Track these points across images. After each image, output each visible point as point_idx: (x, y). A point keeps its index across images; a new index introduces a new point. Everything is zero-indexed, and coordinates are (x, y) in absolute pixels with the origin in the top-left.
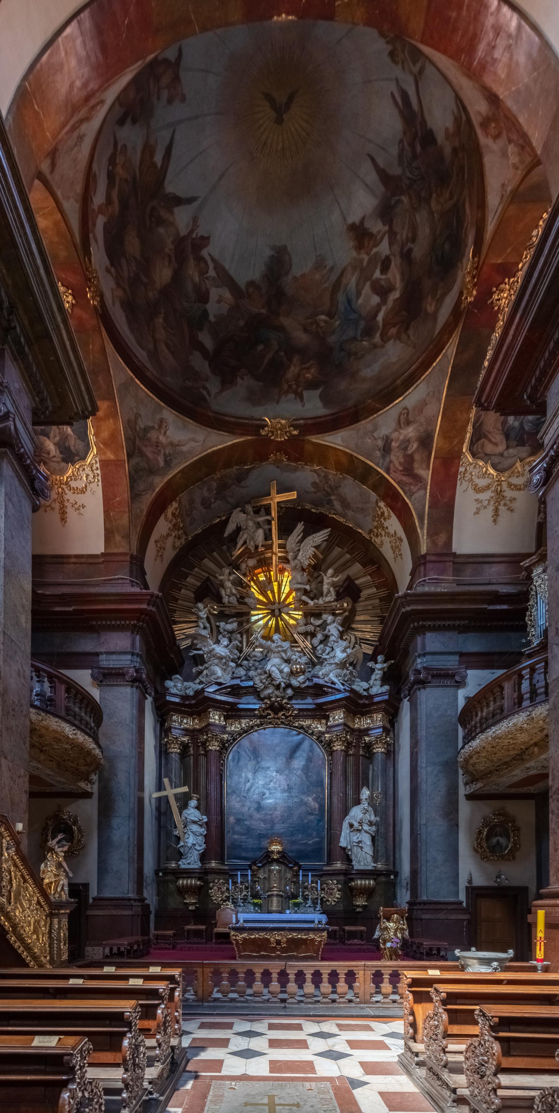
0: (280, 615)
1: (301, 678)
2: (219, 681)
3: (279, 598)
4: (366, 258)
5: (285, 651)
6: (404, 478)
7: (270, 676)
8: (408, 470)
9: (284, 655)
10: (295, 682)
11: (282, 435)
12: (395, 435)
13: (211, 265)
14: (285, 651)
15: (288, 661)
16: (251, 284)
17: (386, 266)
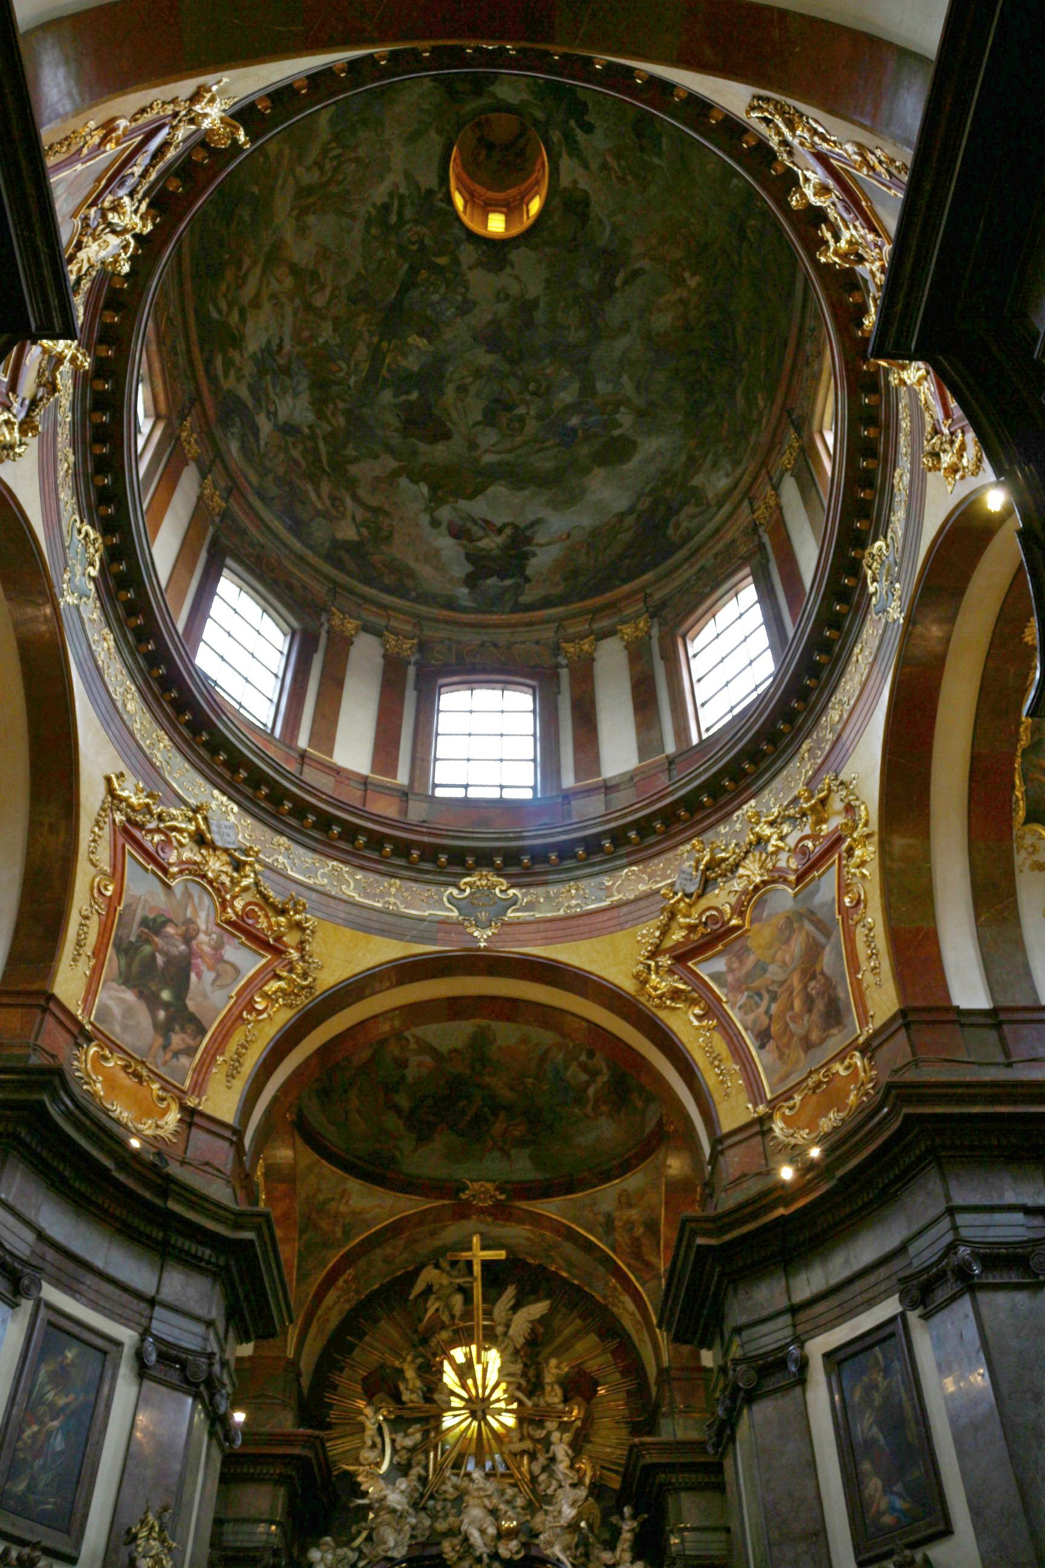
0: (484, 1419)
1: (514, 1544)
2: (390, 1554)
3: (484, 1387)
4: (571, 1045)
5: (489, 1497)
6: (632, 1262)
7: (466, 1539)
8: (636, 1253)
9: (487, 1502)
10: (504, 1552)
11: (485, 1200)
12: (617, 1214)
13: (412, 1040)
14: (489, 1497)
15: (494, 1512)
16: (455, 1051)
17: (591, 1054)
